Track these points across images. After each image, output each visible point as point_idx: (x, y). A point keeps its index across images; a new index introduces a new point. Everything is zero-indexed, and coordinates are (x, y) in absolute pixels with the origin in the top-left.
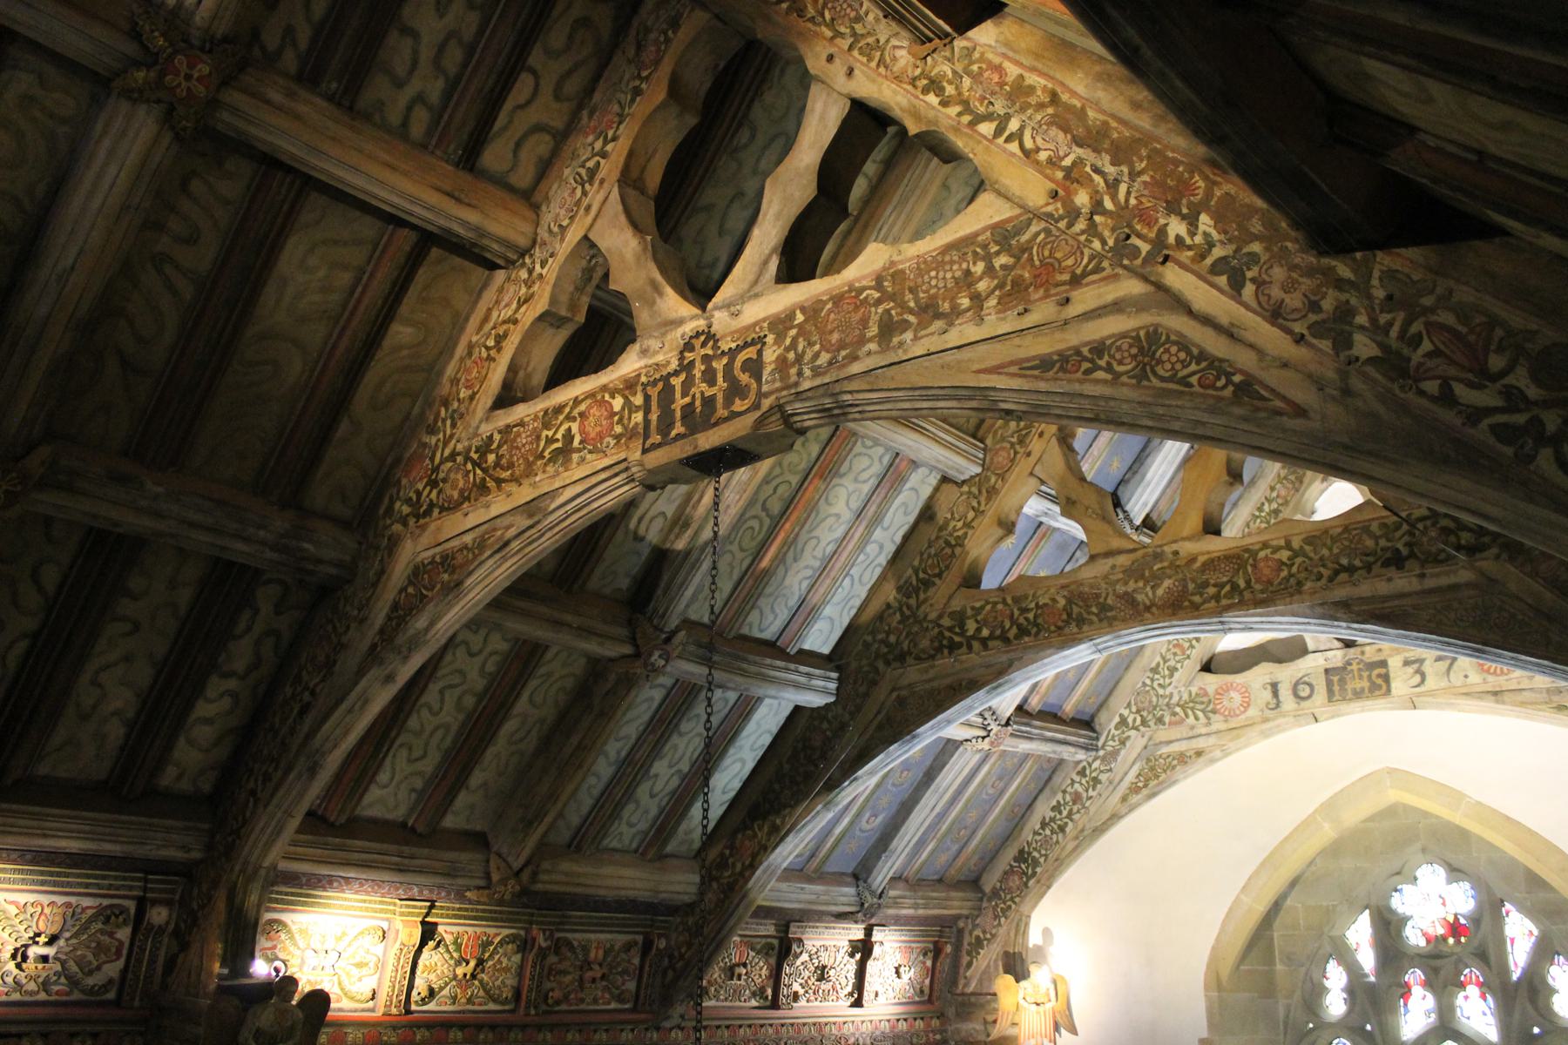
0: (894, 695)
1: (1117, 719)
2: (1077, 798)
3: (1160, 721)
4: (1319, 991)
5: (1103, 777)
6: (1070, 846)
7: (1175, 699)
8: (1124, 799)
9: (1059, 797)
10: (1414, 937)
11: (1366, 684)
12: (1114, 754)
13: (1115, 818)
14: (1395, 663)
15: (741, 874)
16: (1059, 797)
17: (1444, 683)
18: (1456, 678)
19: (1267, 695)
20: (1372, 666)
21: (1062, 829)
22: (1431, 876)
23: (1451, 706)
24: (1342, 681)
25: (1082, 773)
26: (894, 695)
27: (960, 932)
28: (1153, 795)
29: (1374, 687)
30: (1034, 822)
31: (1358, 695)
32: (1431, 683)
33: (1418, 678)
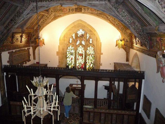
0: (33, 6)
1: (51, 11)
2: (46, 19)
3: (56, 11)
4: (70, 40)
5: (49, 17)
6: (45, 25)
7: (58, 9)
8: (52, 20)
9: (44, 19)
10: (79, 36)
11: (79, 10)
12: (51, 15)
13: (50, 22)
14: (83, 8)
15: (10, 28)
16: (44, 19)
17: (87, 11)
18: (88, 11)
19: (69, 10)
20: (80, 8)
21: (44, 23)
22: (81, 31)
23: (87, 14)
24: (77, 10)
25: (47, 17)
26: (33, 6)
27: (31, 34)
28: (55, 20)
29: (80, 11)
30: (40, 22)
31: (78, 11)
32: (86, 11)
33: (85, 11)
